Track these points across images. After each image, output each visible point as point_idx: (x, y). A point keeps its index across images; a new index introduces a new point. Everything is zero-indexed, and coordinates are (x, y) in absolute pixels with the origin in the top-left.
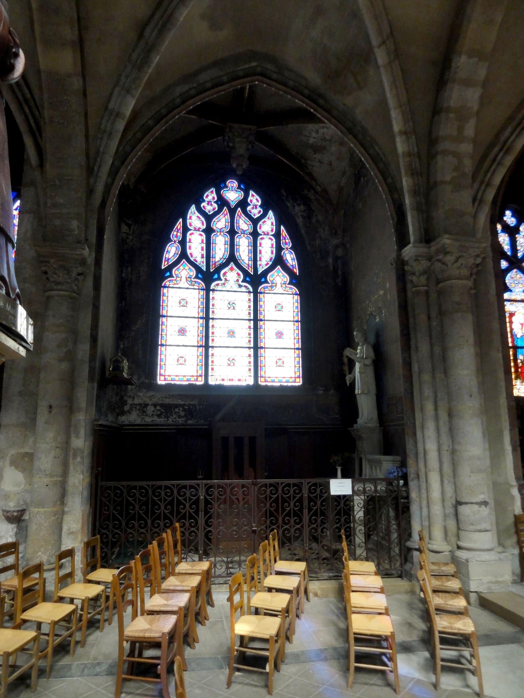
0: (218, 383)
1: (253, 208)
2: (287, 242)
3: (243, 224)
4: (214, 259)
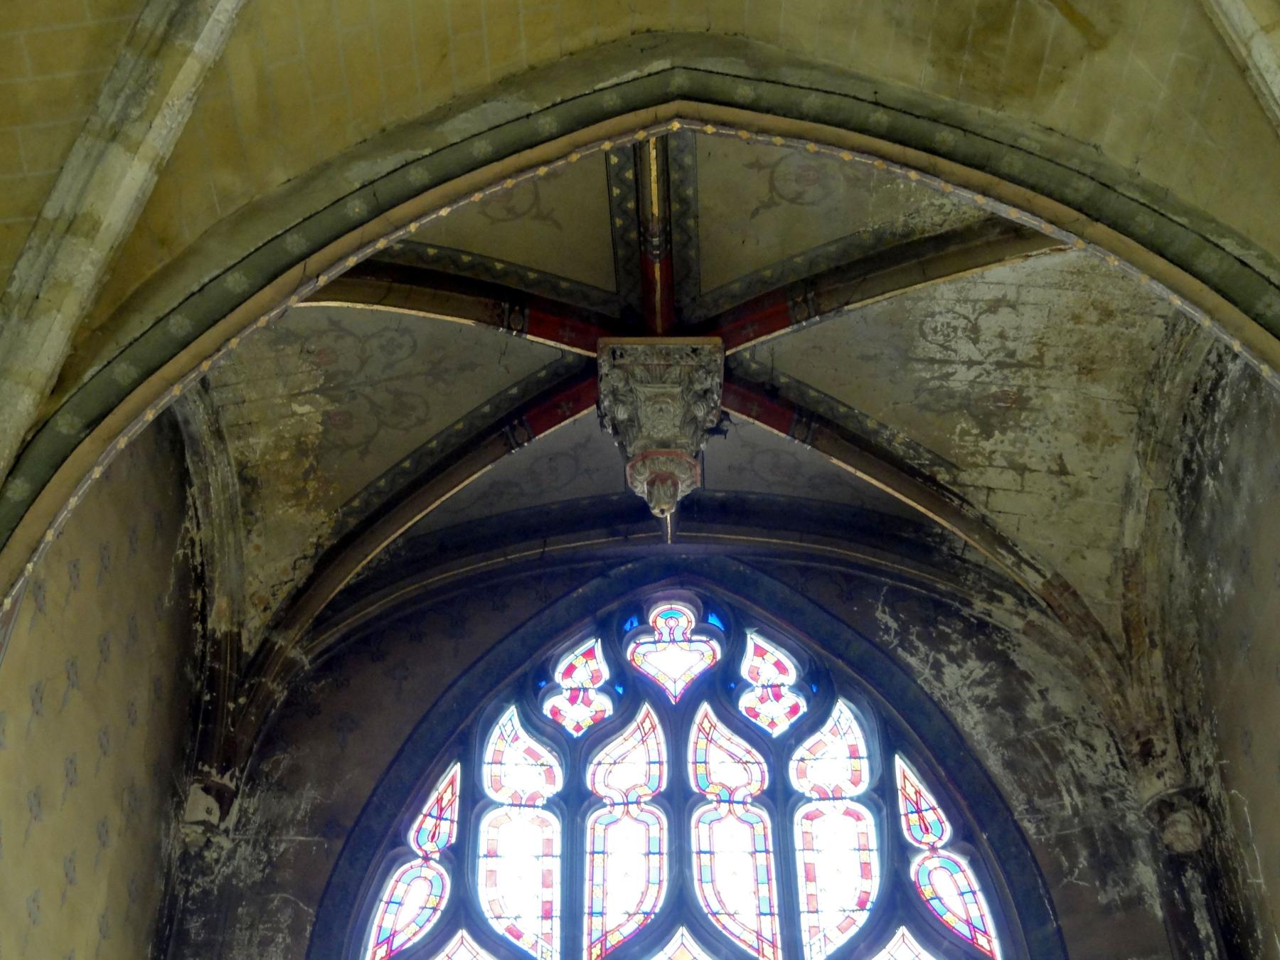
1: (762, 700)
3: (723, 761)
4: (597, 921)
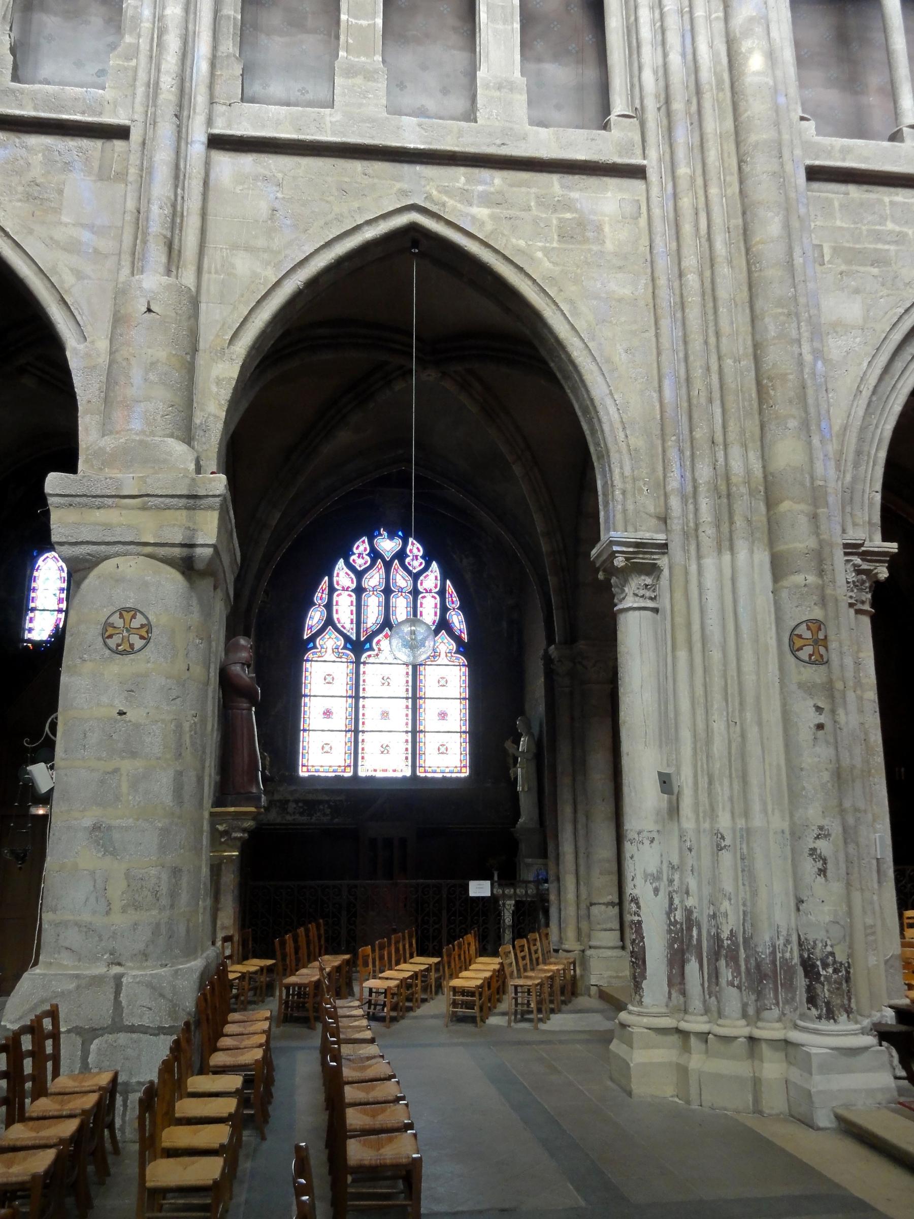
0: (369, 774)
1: (413, 560)
2: (454, 600)
3: (401, 580)
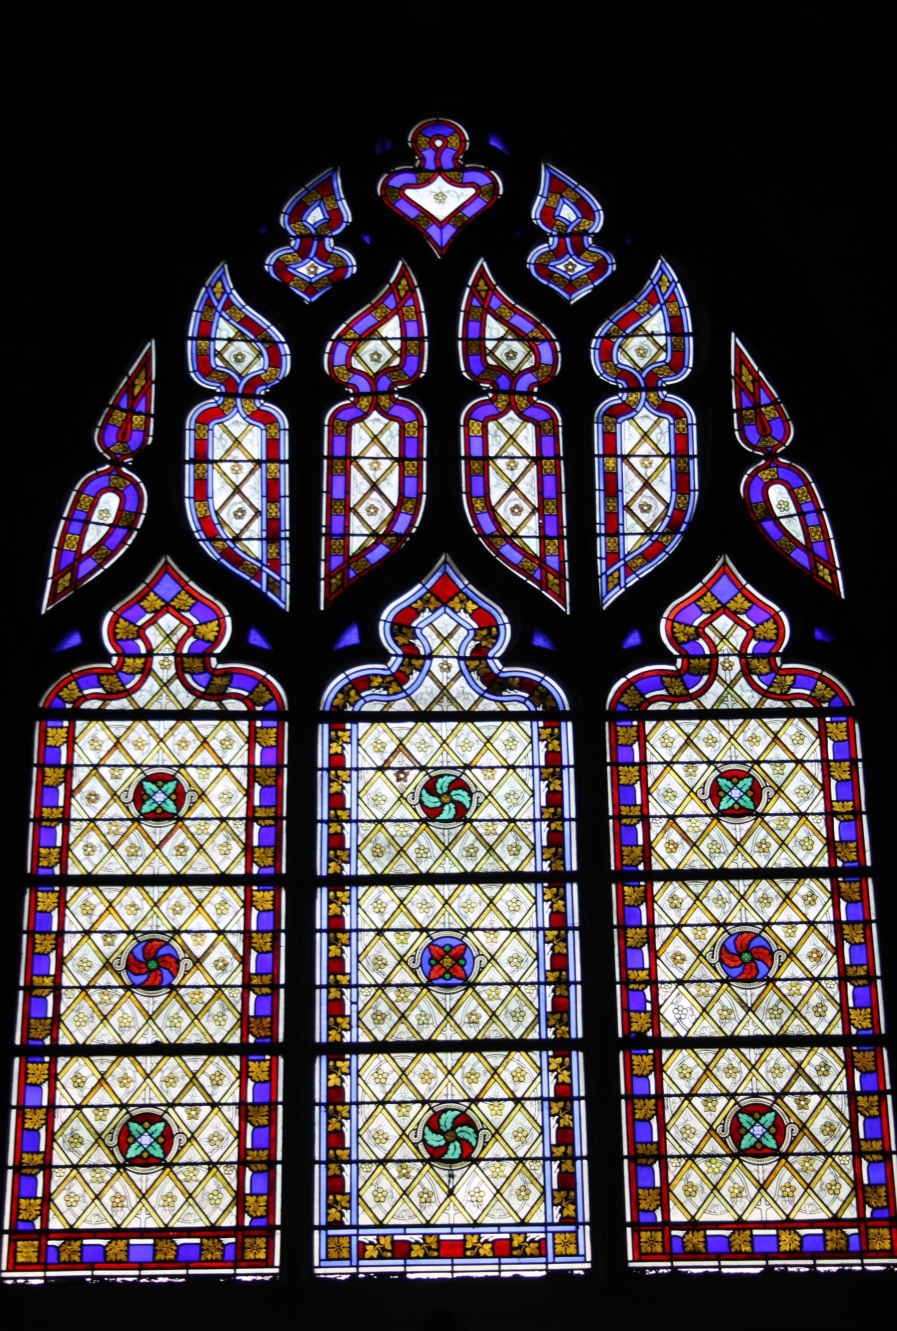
1: (558, 253)
2: (763, 409)
4: (337, 544)
